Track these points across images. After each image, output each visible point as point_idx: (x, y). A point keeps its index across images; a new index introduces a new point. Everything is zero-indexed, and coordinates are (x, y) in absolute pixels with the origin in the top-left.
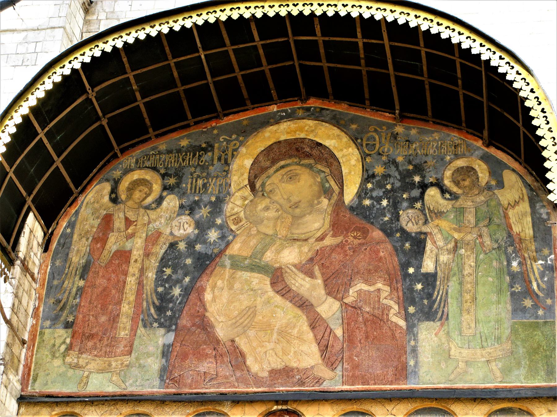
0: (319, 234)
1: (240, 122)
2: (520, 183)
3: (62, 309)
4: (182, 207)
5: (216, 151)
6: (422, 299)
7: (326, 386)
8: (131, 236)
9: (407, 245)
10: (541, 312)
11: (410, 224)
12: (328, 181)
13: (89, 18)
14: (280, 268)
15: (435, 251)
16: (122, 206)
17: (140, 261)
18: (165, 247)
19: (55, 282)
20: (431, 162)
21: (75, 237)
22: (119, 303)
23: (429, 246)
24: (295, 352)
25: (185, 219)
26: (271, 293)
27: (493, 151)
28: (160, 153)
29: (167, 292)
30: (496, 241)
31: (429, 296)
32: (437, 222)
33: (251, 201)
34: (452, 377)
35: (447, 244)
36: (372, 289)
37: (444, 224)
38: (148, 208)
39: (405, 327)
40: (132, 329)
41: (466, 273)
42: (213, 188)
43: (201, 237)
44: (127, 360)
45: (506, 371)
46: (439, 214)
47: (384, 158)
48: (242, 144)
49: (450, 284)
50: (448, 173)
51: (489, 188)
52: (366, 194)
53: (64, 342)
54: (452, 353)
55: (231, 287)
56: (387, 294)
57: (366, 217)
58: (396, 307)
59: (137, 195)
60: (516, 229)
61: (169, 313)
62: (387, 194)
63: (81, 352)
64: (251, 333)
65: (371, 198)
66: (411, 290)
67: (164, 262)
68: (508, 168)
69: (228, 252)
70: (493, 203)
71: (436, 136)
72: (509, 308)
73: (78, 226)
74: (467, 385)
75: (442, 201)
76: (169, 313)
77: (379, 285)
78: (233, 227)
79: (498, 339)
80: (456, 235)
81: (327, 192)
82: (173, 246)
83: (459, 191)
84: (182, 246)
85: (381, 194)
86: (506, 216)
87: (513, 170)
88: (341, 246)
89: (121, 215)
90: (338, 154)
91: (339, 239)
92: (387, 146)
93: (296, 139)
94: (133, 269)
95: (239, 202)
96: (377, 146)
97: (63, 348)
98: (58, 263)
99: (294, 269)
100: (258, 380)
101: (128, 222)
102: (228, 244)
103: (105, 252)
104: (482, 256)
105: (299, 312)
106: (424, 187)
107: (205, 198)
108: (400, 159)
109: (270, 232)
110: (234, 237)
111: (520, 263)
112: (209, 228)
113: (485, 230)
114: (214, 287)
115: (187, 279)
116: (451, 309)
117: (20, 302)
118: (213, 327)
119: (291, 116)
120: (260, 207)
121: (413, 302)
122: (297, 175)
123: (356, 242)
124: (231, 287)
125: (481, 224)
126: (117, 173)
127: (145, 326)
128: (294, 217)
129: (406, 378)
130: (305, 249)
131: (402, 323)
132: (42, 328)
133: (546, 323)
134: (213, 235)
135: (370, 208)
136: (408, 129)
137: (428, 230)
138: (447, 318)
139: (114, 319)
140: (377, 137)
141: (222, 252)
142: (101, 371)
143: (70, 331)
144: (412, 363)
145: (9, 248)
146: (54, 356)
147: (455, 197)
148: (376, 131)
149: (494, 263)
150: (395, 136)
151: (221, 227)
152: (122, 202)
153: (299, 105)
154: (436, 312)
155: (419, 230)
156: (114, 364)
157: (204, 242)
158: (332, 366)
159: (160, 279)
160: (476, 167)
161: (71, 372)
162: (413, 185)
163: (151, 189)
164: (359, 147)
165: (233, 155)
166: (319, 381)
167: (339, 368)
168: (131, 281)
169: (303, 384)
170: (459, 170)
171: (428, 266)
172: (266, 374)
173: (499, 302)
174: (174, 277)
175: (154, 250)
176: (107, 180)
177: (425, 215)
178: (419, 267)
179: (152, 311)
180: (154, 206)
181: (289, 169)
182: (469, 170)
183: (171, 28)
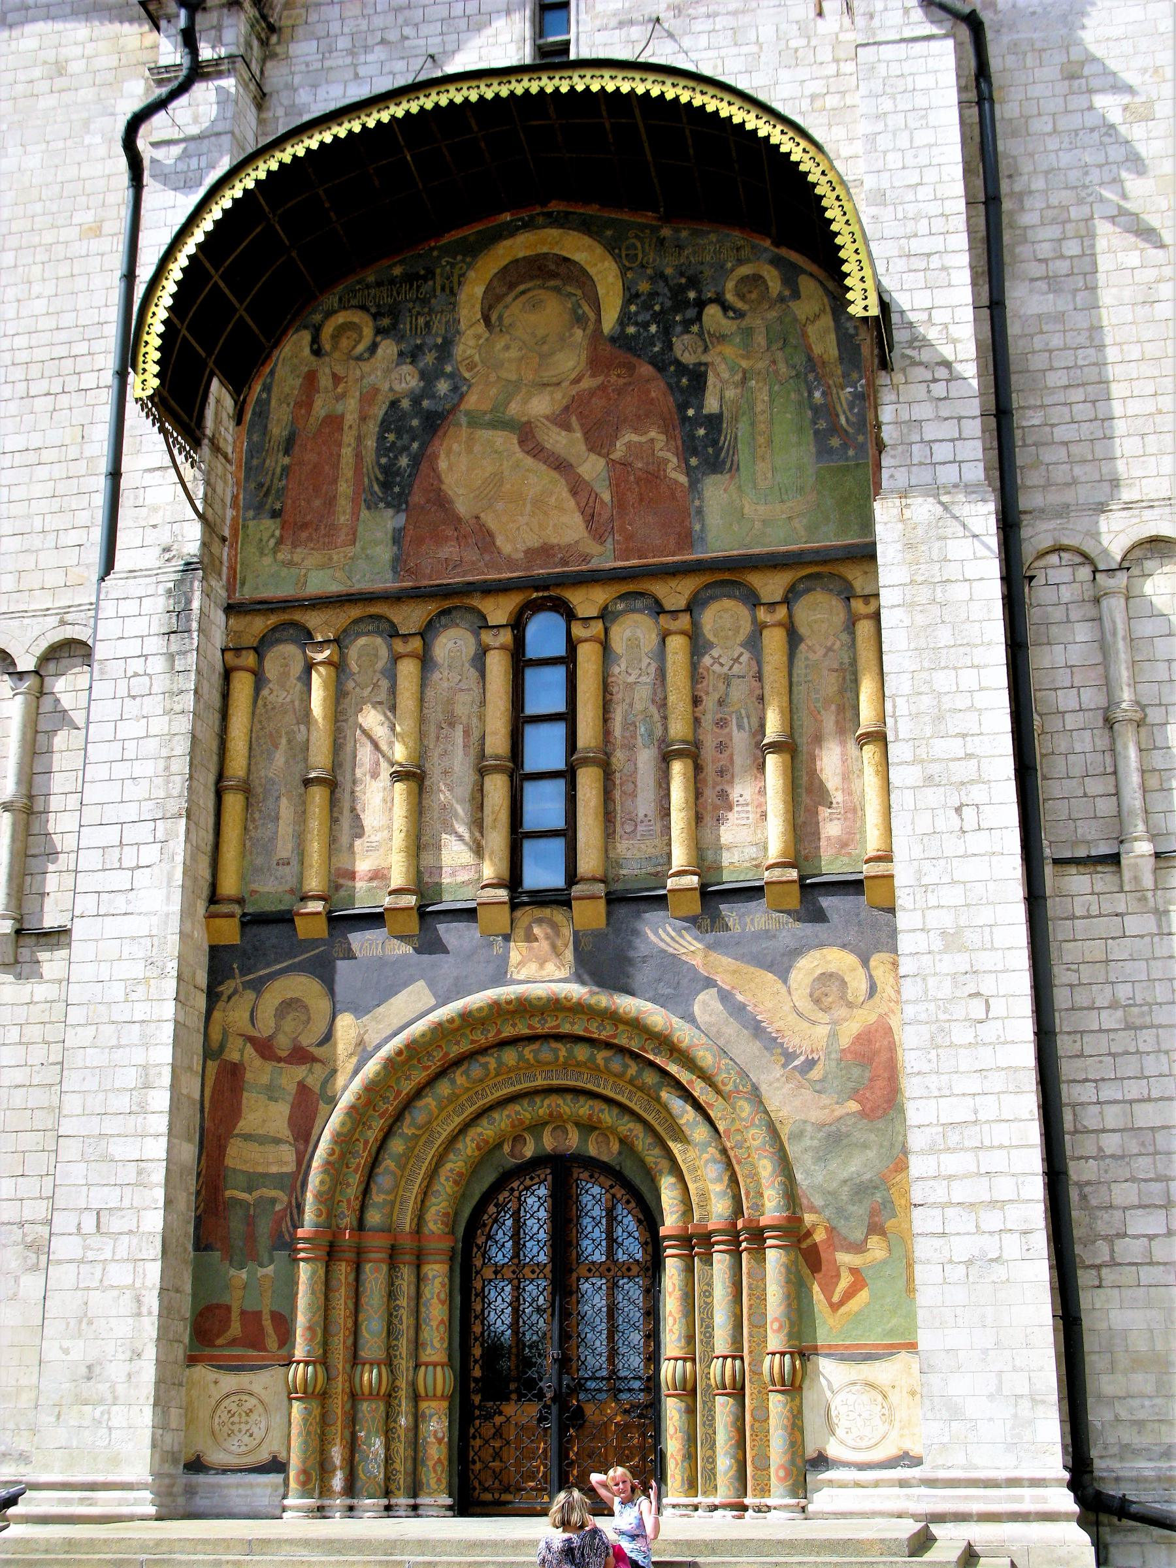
0: (573, 376)
1: (465, 238)
2: (821, 292)
3: (267, 494)
4: (401, 354)
5: (438, 278)
6: (706, 447)
7: (595, 564)
8: (342, 396)
9: (684, 381)
10: (851, 453)
11: (686, 354)
12: (580, 306)
13: (264, 115)
14: (529, 423)
15: (719, 385)
16: (327, 359)
17: (355, 427)
18: (385, 407)
19: (255, 462)
20: (708, 272)
21: (273, 403)
22: (335, 481)
23: (711, 379)
24: (555, 526)
25: (406, 369)
26: (520, 455)
27: (784, 252)
28: (368, 287)
29: (393, 462)
30: (794, 367)
31: (715, 443)
32: (719, 348)
36: (643, 439)
37: (728, 350)
38: (359, 358)
41: (758, 410)
42: (438, 327)
43: (428, 390)
44: (351, 551)
45: (812, 529)
47: (649, 271)
48: (470, 266)
49: (740, 426)
50: (730, 285)
51: (781, 299)
52: (629, 319)
53: (273, 536)
54: (746, 511)
55: (469, 451)
57: (630, 349)
58: (675, 460)
59: (344, 343)
60: (817, 350)
61: (397, 489)
62: (657, 318)
63: (294, 546)
64: (500, 506)
65: (636, 324)
66: (692, 437)
67: (385, 426)
68: (803, 271)
69: (462, 407)
70: (787, 320)
71: (713, 237)
72: (813, 450)
73: (275, 389)
74: (765, 550)
75: (724, 322)
76: (397, 489)
77: (653, 434)
78: (467, 375)
79: (801, 490)
80: (745, 364)
81: (579, 320)
82: (394, 404)
83: (745, 307)
84: (405, 404)
85: (648, 317)
86: (804, 335)
87: (811, 275)
88: (602, 388)
89: (327, 370)
90: (592, 271)
92: (651, 257)
93: (538, 255)
94: (349, 438)
95: (472, 343)
96: (640, 256)
97: (272, 542)
98: (255, 438)
100: (511, 563)
101: (336, 379)
102: (462, 396)
103: (312, 420)
104: (776, 388)
105: (555, 475)
106: (701, 304)
107: (430, 341)
108: (669, 271)
109: (513, 377)
110: (469, 387)
111: (824, 394)
112: (437, 378)
113: (779, 354)
114: (449, 453)
115: (415, 445)
116: (741, 457)
117: (214, 490)
118: (451, 502)
119: (529, 225)
120: (500, 345)
121: (695, 452)
123: (621, 381)
124: (469, 451)
125: (774, 347)
126: (317, 318)
127: (369, 508)
128: (542, 356)
129: (692, 546)
130: (558, 395)
131: (683, 479)
132: (245, 520)
133: (857, 465)
134: (443, 387)
135: (635, 337)
136: (677, 231)
138: (738, 469)
139: (331, 502)
140: (639, 245)
141: (455, 408)
142: (322, 567)
143: (278, 520)
144: (697, 527)
145: (193, 425)
146: (262, 554)
147: (740, 315)
148: (637, 237)
149: (793, 395)
150: (661, 242)
151: (451, 376)
152: (327, 354)
153: (538, 210)
154: (724, 462)
156: (335, 557)
157: (433, 396)
158: (599, 538)
159: (383, 448)
160: (765, 274)
161: (284, 572)
162: (686, 303)
163: (361, 337)
164: (617, 258)
165: (460, 283)
166: (586, 558)
167: (610, 540)
168: (347, 453)
169: (566, 564)
170: (744, 280)
171: (711, 405)
172: (522, 555)
173: (799, 444)
174: (399, 444)
175: (371, 412)
176: (306, 327)
177: (704, 340)
178: (700, 407)
179: (376, 488)
180: (366, 355)
181: (531, 294)
182: (757, 279)
183: (364, 125)
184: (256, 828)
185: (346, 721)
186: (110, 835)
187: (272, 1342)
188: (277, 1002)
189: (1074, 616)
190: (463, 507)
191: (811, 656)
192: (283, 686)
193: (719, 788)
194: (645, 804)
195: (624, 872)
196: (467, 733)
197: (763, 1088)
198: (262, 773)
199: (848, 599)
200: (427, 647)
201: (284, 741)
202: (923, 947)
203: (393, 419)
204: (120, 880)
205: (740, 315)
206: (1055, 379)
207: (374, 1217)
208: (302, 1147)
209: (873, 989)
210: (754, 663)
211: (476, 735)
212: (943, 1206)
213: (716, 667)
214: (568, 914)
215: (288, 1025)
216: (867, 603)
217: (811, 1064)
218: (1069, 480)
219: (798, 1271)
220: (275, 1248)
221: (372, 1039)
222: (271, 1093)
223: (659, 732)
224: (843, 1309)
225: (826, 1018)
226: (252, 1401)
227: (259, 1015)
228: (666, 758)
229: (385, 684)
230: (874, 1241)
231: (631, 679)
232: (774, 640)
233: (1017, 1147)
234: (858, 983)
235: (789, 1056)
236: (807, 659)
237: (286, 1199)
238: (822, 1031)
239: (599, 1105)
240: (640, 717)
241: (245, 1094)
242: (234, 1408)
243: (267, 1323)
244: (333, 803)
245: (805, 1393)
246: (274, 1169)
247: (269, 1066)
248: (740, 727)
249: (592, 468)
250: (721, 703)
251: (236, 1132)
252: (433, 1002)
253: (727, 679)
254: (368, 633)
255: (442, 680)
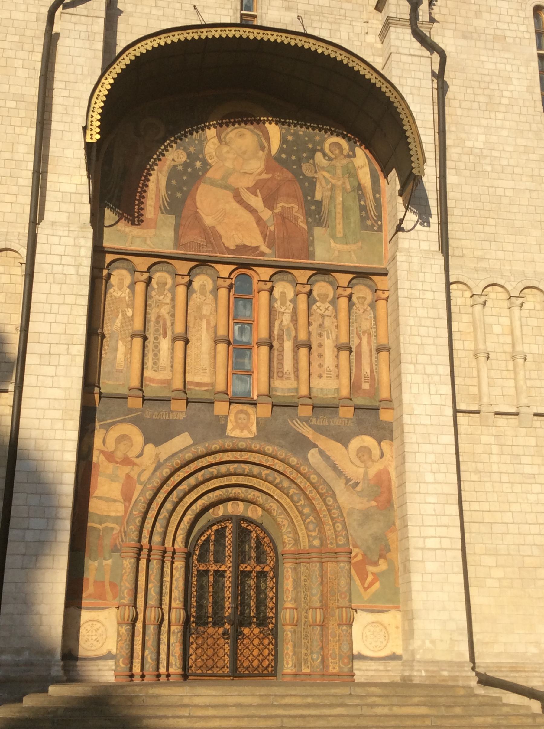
0: (259, 171)
9: (307, 184)
10: (375, 228)
11: (307, 172)
14: (238, 189)
31: (319, 213)
33: (218, 146)
34: (332, 258)
35: (327, 185)
39: (307, 229)
40: (154, 215)
46: (323, 168)
56: (297, 210)
58: (302, 217)
60: (362, 181)
77: (292, 205)
78: (210, 161)
83: (333, 156)
84: (180, 168)
91: (269, 176)
95: (212, 146)
99: (246, 190)
104: (345, 194)
106: (314, 151)
110: (211, 167)
121: (310, 216)
122: (244, 134)
131: (306, 228)
137: (317, 176)
147: (330, 159)
155: (312, 176)
158: (269, 247)
159: (168, 186)
166: (263, 254)
170: (332, 144)
171: (318, 196)
178: (313, 196)
183: (200, 36)
184: (106, 353)
185: (151, 310)
186: (45, 348)
187: (110, 596)
188: (116, 435)
189: (462, 311)
190: (209, 221)
191: (357, 311)
192: (120, 290)
193: (318, 363)
194: (288, 365)
195: (279, 394)
196: (208, 323)
197: (337, 492)
198: (109, 328)
199: (376, 290)
200: (190, 282)
201: (120, 315)
202: (414, 440)
203: (174, 173)
204: (50, 370)
205: (330, 159)
206: (457, 212)
207: (157, 539)
208: (127, 504)
209: (382, 455)
210: (334, 311)
211: (213, 324)
212: (422, 549)
213: (318, 310)
214: (255, 409)
215: (122, 447)
216: (384, 293)
217: (357, 484)
218: (461, 254)
219: (350, 573)
220: (113, 551)
221: (163, 457)
222: (113, 478)
223: (293, 334)
224: (369, 590)
225: (362, 465)
226: (98, 625)
227: (108, 441)
228: (297, 346)
229: (169, 295)
230: (381, 561)
231: (282, 310)
232: (343, 303)
233: (440, 526)
234: (376, 452)
235: (348, 480)
236: (356, 313)
237: (119, 528)
238: (362, 470)
239: (257, 493)
240: (286, 327)
241: (99, 478)
242: (89, 628)
243: (108, 587)
244: (144, 347)
245: (353, 627)
246: (113, 514)
247: (111, 466)
248: (328, 338)
249: (266, 214)
250: (320, 326)
251: (94, 495)
252: (192, 442)
253: (323, 316)
254: (162, 271)
255: (196, 298)
